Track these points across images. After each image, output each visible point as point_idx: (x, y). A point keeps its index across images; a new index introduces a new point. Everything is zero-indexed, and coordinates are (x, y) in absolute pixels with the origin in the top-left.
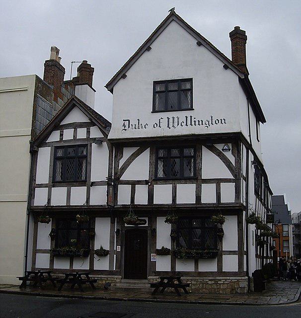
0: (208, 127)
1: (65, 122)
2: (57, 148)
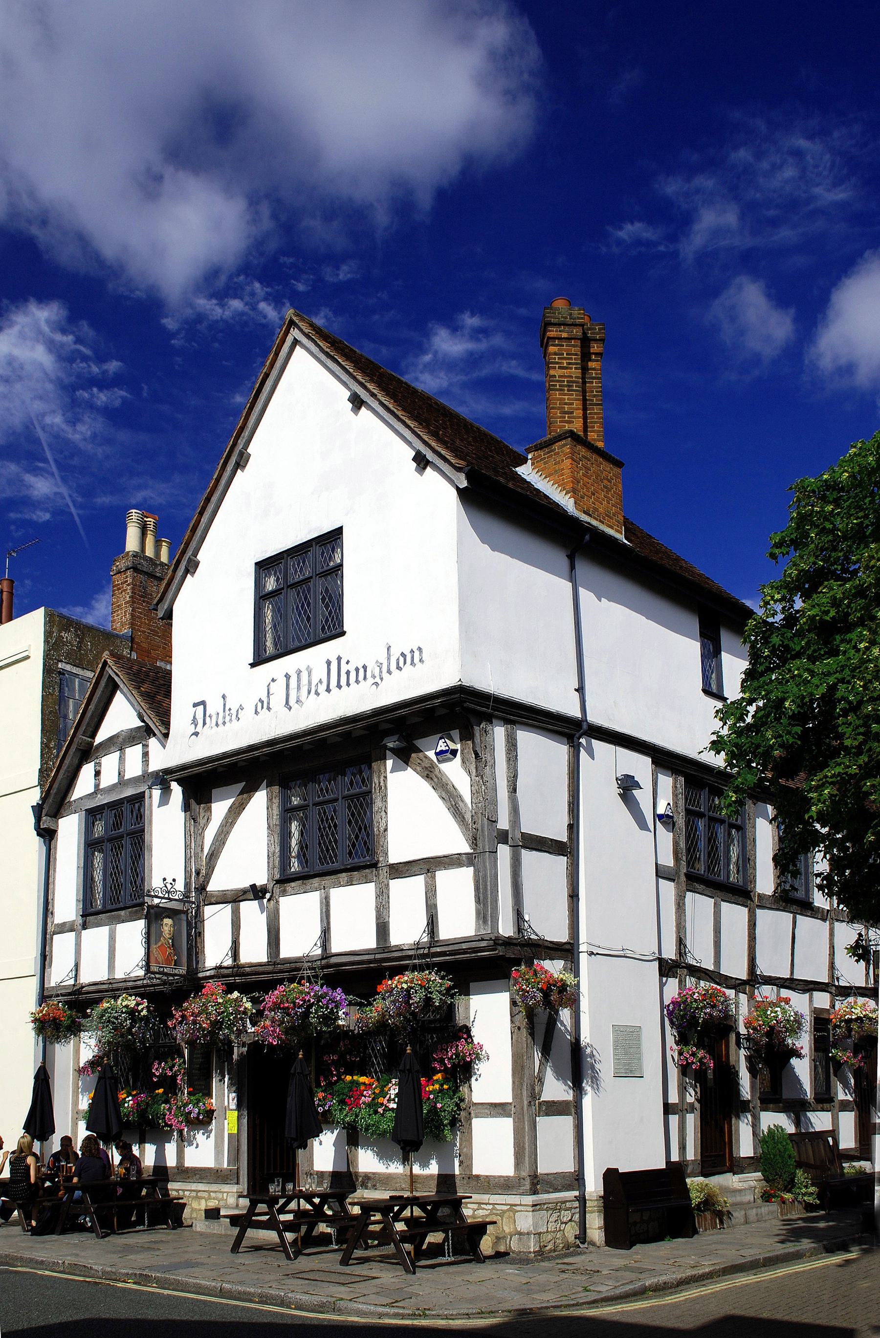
0: (376, 684)
1: (102, 736)
2: (93, 814)
